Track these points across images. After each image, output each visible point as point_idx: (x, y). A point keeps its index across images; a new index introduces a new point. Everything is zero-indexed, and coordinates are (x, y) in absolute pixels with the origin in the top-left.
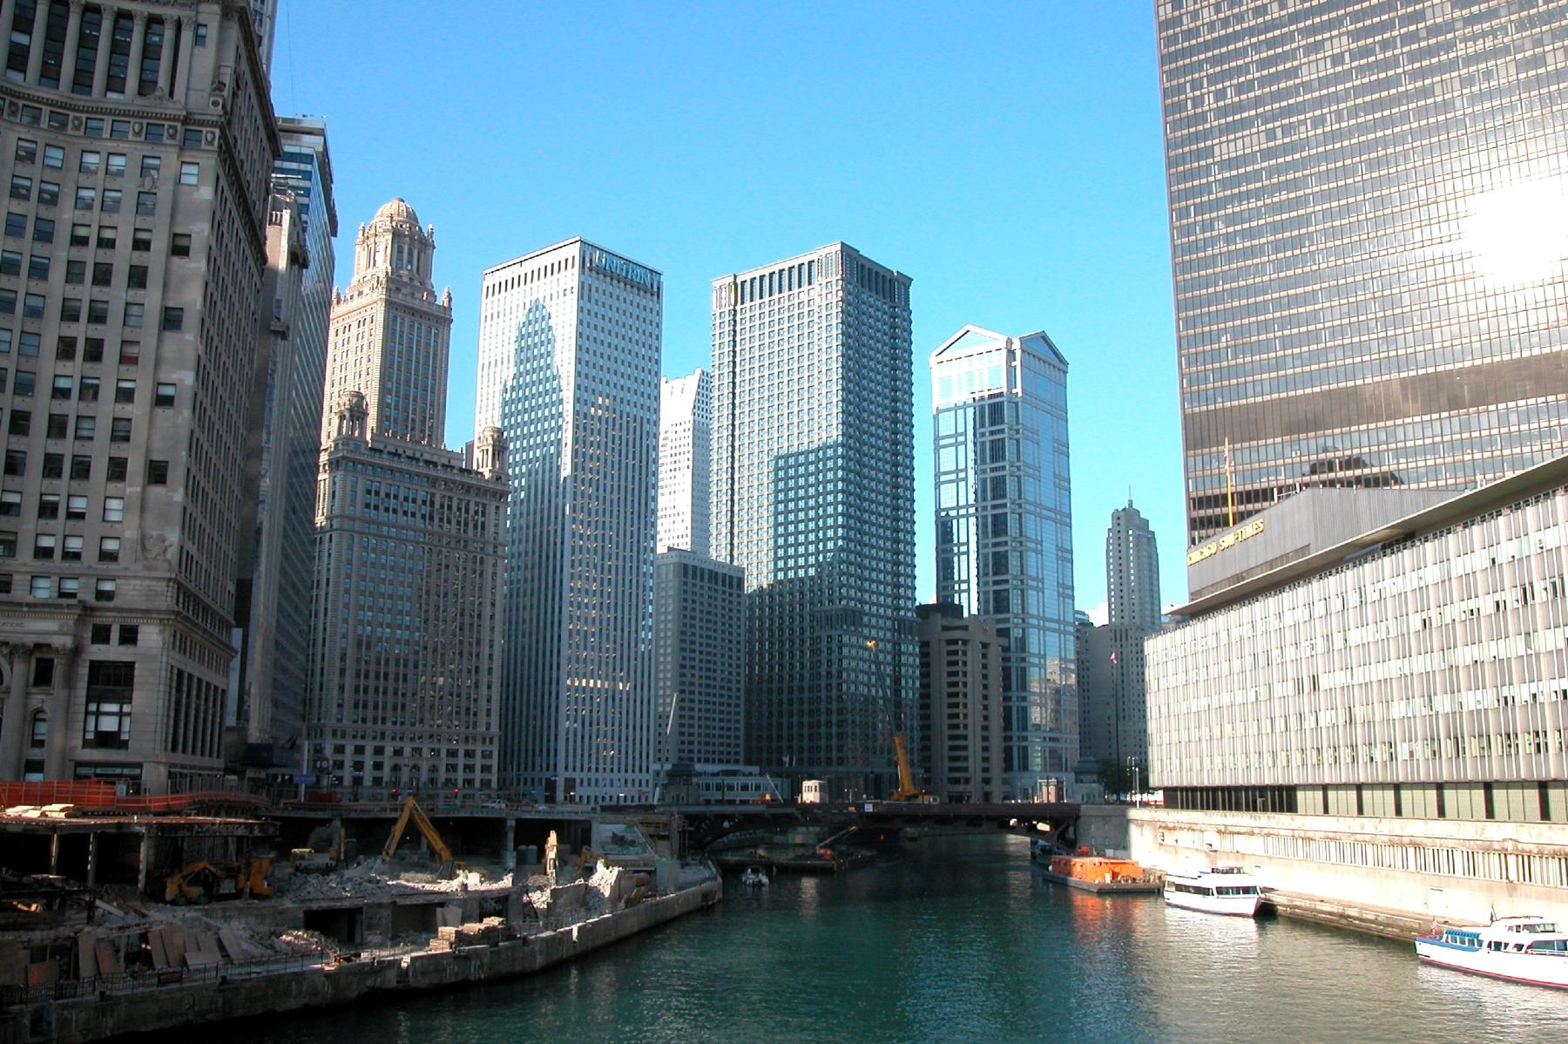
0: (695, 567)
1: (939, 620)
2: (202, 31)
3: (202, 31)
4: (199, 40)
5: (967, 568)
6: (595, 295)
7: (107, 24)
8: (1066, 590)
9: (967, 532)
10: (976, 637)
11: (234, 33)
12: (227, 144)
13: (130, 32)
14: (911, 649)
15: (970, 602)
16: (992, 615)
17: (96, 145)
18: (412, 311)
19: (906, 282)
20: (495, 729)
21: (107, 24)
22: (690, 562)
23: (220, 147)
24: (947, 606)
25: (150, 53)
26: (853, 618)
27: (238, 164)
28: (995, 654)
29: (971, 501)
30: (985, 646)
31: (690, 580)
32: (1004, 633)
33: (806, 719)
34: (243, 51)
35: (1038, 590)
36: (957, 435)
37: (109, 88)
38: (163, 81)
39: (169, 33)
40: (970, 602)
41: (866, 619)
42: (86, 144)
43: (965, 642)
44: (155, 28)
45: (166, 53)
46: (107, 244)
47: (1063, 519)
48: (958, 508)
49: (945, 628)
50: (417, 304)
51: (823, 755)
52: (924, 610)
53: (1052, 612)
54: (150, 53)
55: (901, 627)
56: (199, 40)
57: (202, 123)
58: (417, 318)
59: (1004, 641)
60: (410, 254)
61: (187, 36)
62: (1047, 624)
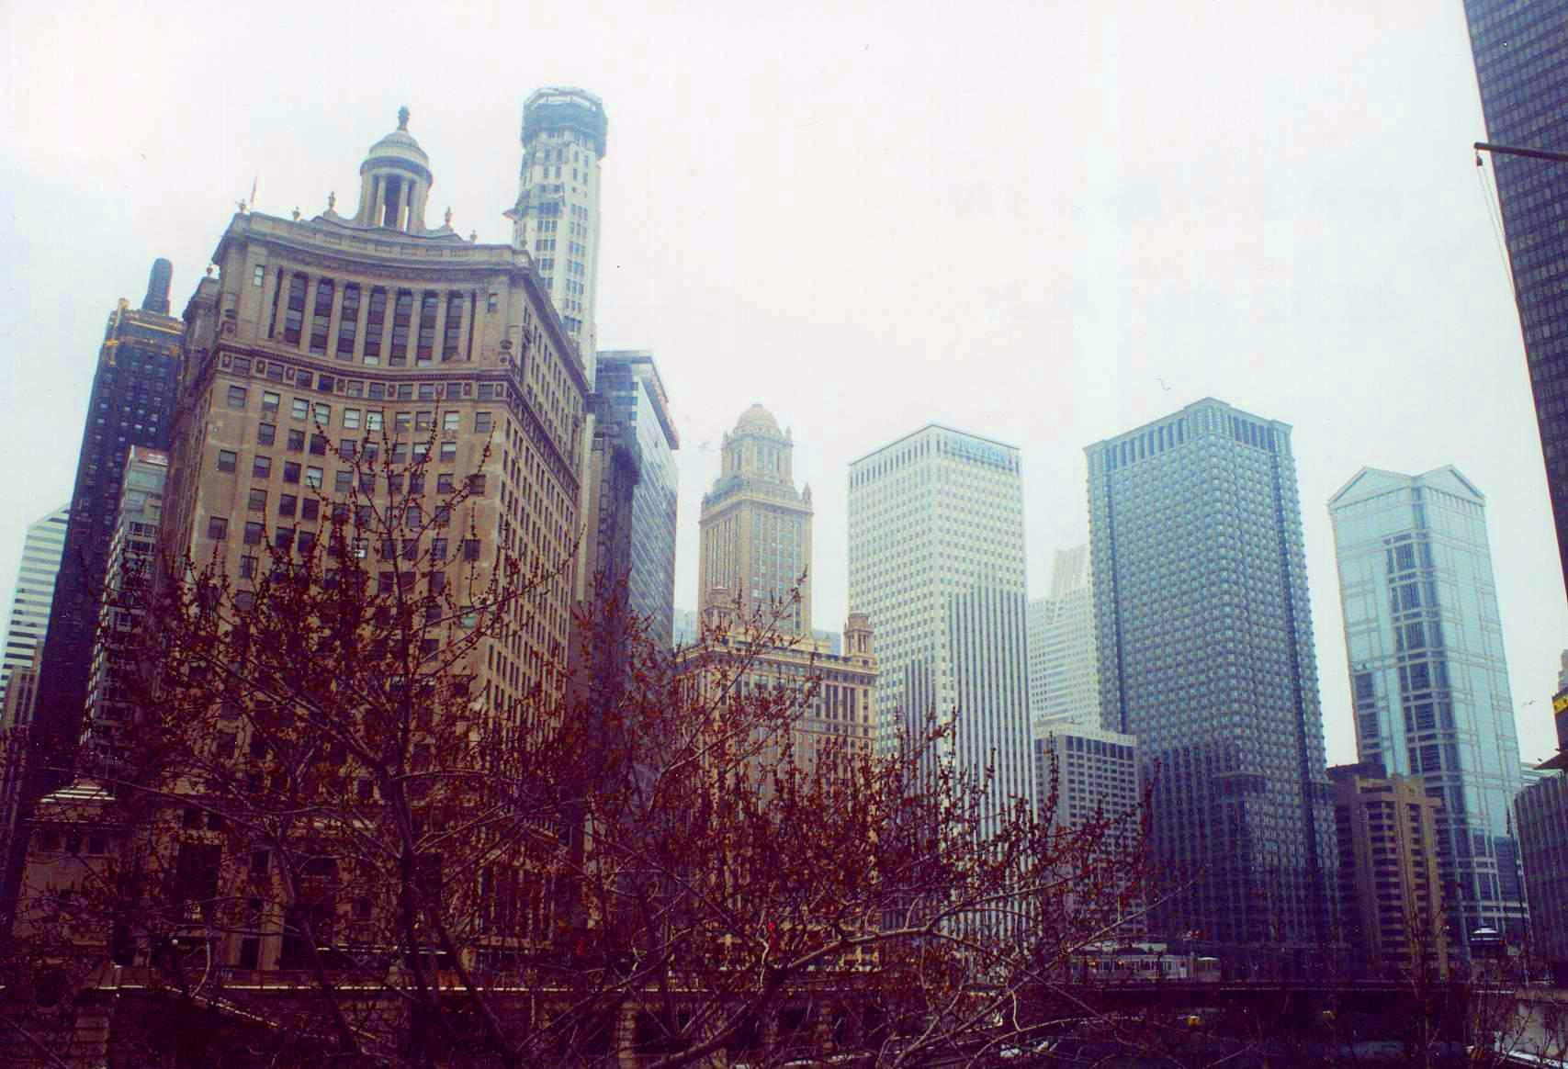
0: (1080, 740)
1: (1360, 783)
2: (493, 300)
3: (493, 300)
4: (491, 308)
5: (1392, 722)
6: (953, 477)
8: (1506, 741)
9: (1388, 686)
10: (1402, 797)
11: (522, 299)
12: (520, 397)
13: (435, 307)
14: (1325, 815)
15: (1397, 761)
16: (1422, 775)
17: (407, 407)
18: (775, 509)
19: (1286, 430)
22: (1075, 734)
23: (510, 395)
24: (1371, 764)
26: (1257, 785)
27: (535, 410)
30: (1414, 807)
31: (1075, 752)
32: (1435, 792)
33: (1212, 893)
34: (532, 309)
35: (1469, 743)
37: (419, 358)
39: (467, 305)
40: (1397, 761)
41: (1269, 785)
42: (399, 407)
43: (1390, 805)
44: (456, 301)
45: (465, 322)
47: (1495, 665)
48: (1373, 659)
49: (1365, 790)
50: (778, 501)
51: (1233, 931)
52: (1339, 773)
53: (1491, 765)
54: (452, 324)
55: (1309, 791)
56: (491, 308)
57: (492, 378)
58: (779, 515)
59: (1437, 802)
60: (770, 455)
61: (481, 306)
62: (1489, 781)
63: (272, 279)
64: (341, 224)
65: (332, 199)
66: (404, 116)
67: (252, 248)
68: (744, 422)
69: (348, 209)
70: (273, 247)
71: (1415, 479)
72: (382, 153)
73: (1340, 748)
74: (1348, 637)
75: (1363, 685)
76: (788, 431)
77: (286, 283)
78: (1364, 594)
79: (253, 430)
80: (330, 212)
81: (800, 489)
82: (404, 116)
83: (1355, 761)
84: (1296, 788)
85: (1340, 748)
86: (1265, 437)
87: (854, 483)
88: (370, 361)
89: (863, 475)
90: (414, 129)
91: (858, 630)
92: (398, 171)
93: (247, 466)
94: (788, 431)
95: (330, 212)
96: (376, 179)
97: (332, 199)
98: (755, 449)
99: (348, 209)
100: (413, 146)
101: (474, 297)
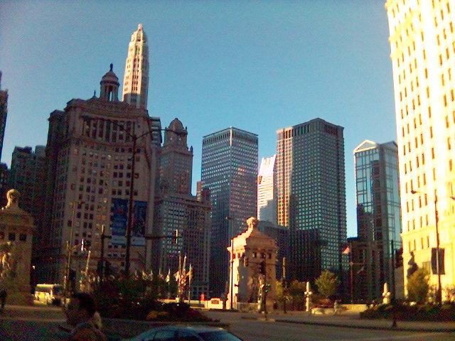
4: (139, 126)
20: (208, 281)
26: (325, 243)
28: (378, 256)
29: (369, 200)
36: (363, 178)
48: (364, 203)
52: (351, 240)
61: (136, 125)
66: (112, 66)
67: (77, 109)
69: (98, 96)
71: (381, 145)
72: (107, 79)
73: (352, 231)
74: (357, 195)
75: (360, 209)
78: (363, 181)
80: (94, 97)
81: (189, 147)
82: (112, 66)
83: (356, 235)
84: (337, 245)
85: (352, 231)
86: (336, 132)
87: (204, 143)
90: (114, 70)
91: (206, 193)
92: (112, 85)
93: (79, 170)
96: (106, 87)
100: (114, 76)
101: (134, 123)
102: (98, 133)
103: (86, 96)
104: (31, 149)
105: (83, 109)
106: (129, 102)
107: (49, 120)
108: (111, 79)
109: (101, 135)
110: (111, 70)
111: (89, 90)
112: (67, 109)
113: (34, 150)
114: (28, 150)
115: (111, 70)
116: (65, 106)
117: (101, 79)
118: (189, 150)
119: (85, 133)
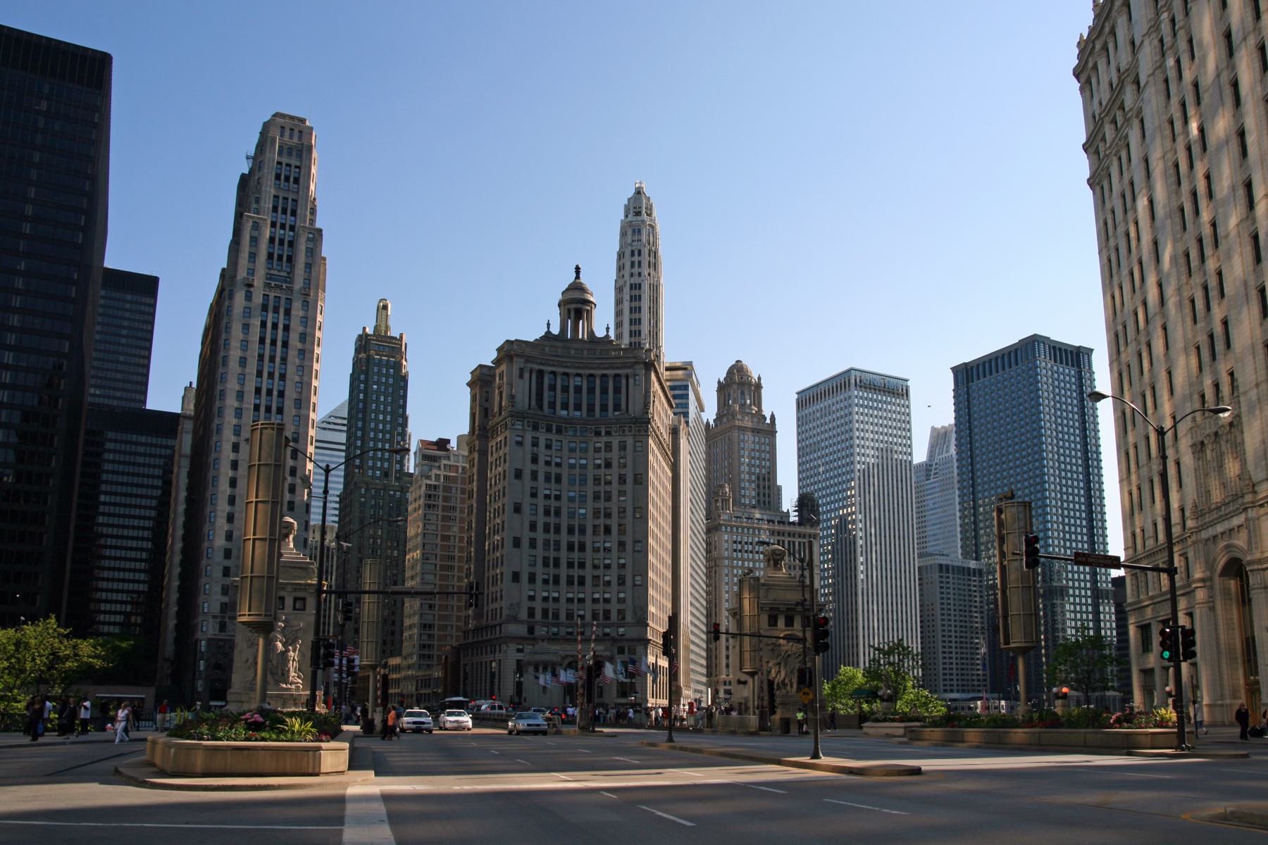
7: (598, 382)
17: (600, 439)
21: (598, 382)
25: (617, 390)
38: (623, 407)
39: (624, 381)
46: (609, 483)
54: (617, 390)
61: (631, 381)
63: (527, 375)
64: (555, 338)
65: (548, 325)
66: (578, 269)
68: (730, 372)
69: (555, 330)
70: (528, 360)
76: (759, 378)
77: (534, 376)
79: (529, 457)
80: (548, 332)
82: (578, 269)
88: (578, 413)
89: (806, 399)
90: (584, 279)
91: (806, 503)
92: (579, 306)
94: (759, 378)
95: (548, 332)
96: (569, 310)
97: (548, 325)
98: (739, 386)
99: (555, 330)
101: (627, 377)
102: (274, 408)
103: (532, 333)
104: (448, 441)
105: (528, 360)
106: (612, 335)
107: (470, 384)
108: (576, 295)
109: (565, 406)
110: (578, 277)
111: (537, 319)
112: (497, 362)
113: (453, 444)
114: (442, 444)
115: (578, 277)
116: (494, 355)
117: (560, 297)
118: (768, 421)
119: (533, 402)
